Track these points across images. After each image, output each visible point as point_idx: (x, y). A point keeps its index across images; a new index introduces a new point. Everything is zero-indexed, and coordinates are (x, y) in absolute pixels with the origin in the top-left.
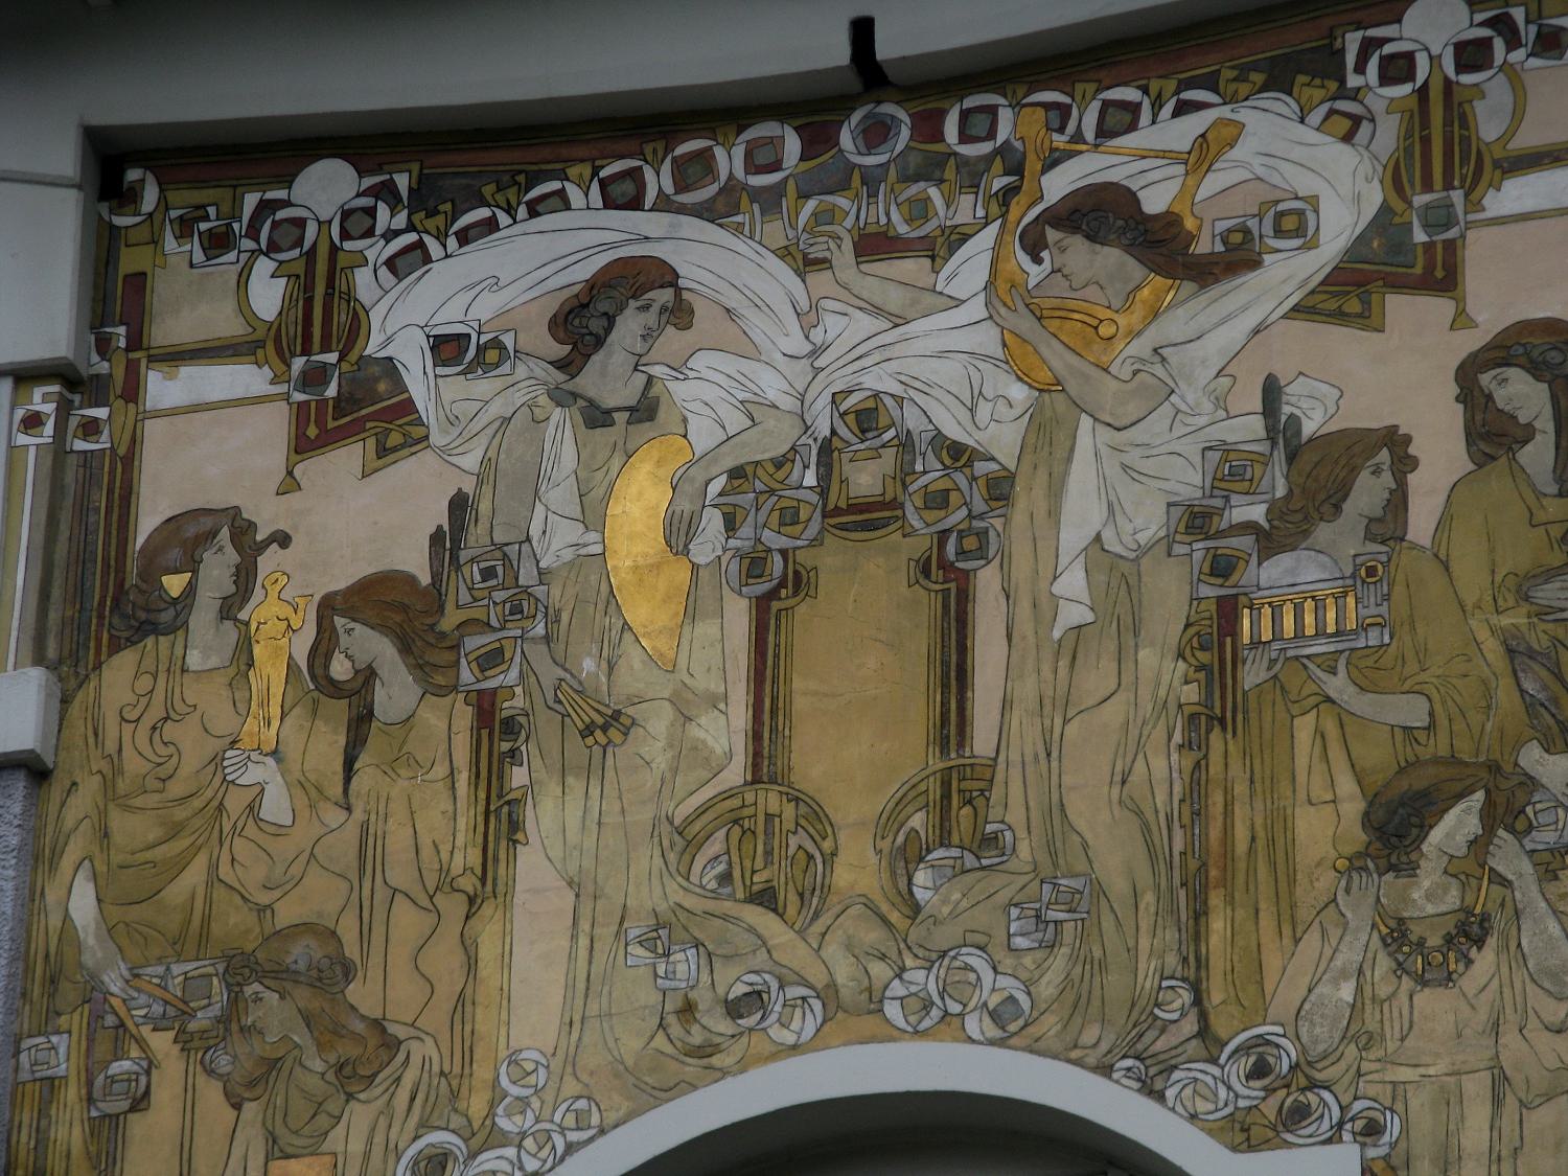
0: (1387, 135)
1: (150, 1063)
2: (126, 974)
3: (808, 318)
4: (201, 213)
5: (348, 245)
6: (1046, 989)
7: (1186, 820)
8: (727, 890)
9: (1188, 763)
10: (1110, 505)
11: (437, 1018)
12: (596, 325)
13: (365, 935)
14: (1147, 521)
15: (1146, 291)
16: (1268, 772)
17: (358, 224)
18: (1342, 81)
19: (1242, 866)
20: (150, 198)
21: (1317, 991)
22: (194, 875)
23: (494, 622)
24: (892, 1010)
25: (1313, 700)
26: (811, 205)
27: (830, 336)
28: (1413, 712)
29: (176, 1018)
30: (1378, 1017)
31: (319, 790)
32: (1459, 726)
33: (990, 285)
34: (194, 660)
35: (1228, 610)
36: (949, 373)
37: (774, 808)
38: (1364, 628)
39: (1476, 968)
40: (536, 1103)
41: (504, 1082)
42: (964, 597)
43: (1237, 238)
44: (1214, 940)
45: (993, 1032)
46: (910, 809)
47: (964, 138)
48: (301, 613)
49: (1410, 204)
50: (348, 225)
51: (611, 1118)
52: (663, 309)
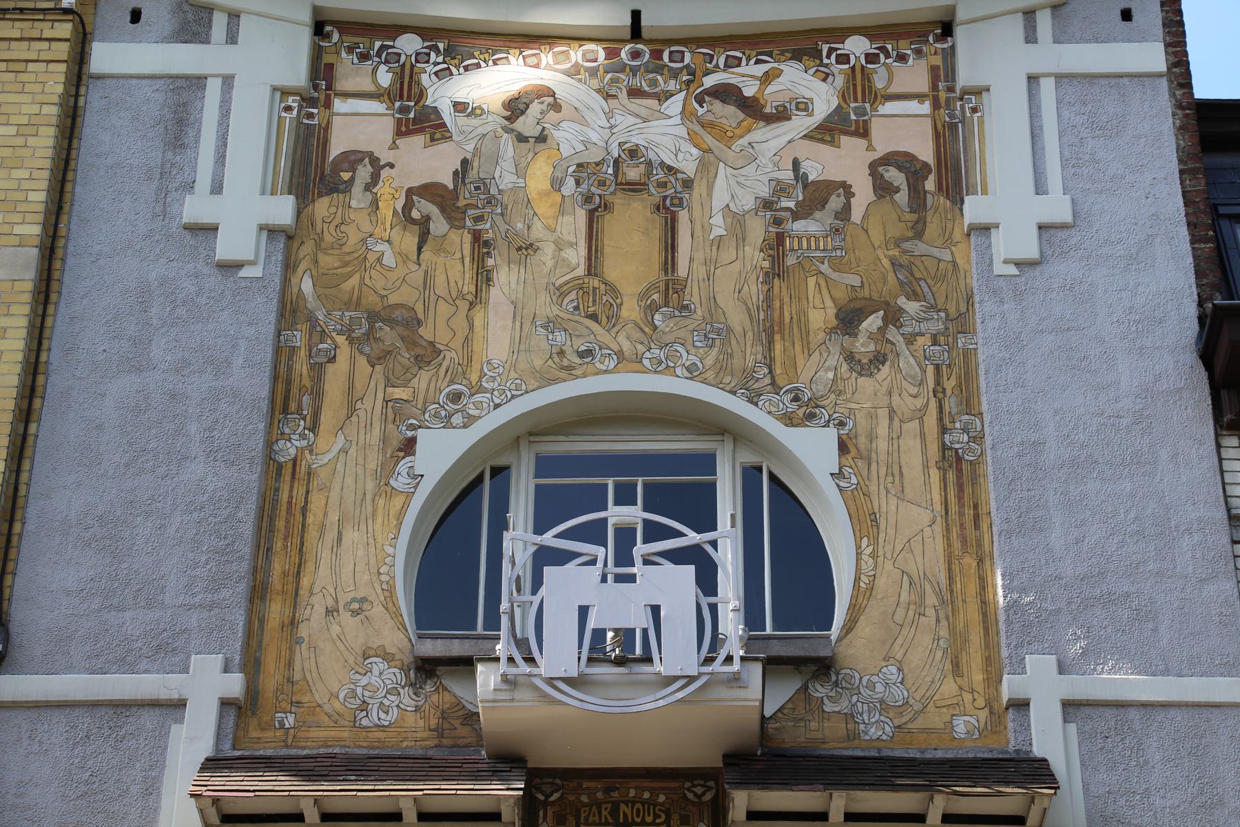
0: (840, 81)
1: (336, 346)
2: (325, 313)
3: (609, 115)
4: (357, 46)
5: (418, 65)
6: (709, 361)
7: (765, 308)
8: (578, 312)
9: (766, 288)
10: (732, 195)
11: (457, 343)
12: (522, 107)
13: (426, 310)
14: (747, 202)
15: (745, 123)
16: (797, 296)
18: (822, 61)
19: (787, 327)
20: (336, 37)
21: (819, 373)
22: (354, 281)
23: (480, 206)
24: (646, 362)
25: (814, 272)
26: (609, 76)
27: (617, 123)
28: (856, 281)
29: (348, 331)
30: (843, 385)
31: (407, 257)
32: (873, 287)
33: (683, 112)
34: (354, 204)
35: (780, 238)
36: (667, 141)
37: (596, 284)
39: (881, 372)
40: (498, 378)
41: (485, 370)
43: (781, 109)
44: (777, 352)
45: (690, 375)
46: (652, 292)
47: (671, 61)
48: (399, 193)
49: (849, 106)
50: (418, 58)
51: (530, 388)
52: (549, 105)
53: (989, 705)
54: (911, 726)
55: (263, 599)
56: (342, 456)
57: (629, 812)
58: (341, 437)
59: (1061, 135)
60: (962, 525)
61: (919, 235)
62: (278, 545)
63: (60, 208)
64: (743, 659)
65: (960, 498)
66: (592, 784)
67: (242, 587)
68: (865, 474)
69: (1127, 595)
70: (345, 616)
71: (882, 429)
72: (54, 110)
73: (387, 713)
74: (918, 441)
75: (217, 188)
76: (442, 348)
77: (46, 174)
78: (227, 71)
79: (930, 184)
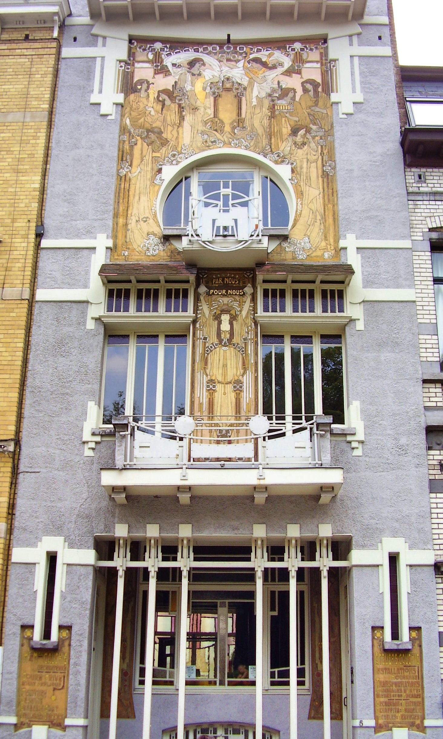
0: (292, 57)
3: (220, 67)
6: (252, 144)
9: (269, 121)
11: (174, 139)
13: (164, 129)
14: (263, 94)
17: (162, 50)
20: (135, 44)
22: (142, 120)
24: (232, 144)
26: (220, 55)
28: (297, 119)
33: (243, 66)
35: (274, 106)
36: (239, 75)
38: (290, 109)
42: (241, 100)
47: (240, 50)
53: (335, 249)
54: (312, 255)
55: (117, 217)
56: (140, 174)
57: (227, 280)
58: (139, 168)
59: (360, 74)
60: (328, 195)
61: (316, 105)
62: (121, 201)
63: (54, 99)
64: (262, 235)
65: (328, 187)
66: (217, 272)
67: (111, 214)
68: (299, 179)
69: (377, 216)
70: (142, 222)
71: (305, 165)
72: (51, 69)
73: (155, 251)
74: (316, 169)
75: (100, 92)
76: (169, 140)
77: (49, 89)
78: (103, 56)
79: (320, 89)
